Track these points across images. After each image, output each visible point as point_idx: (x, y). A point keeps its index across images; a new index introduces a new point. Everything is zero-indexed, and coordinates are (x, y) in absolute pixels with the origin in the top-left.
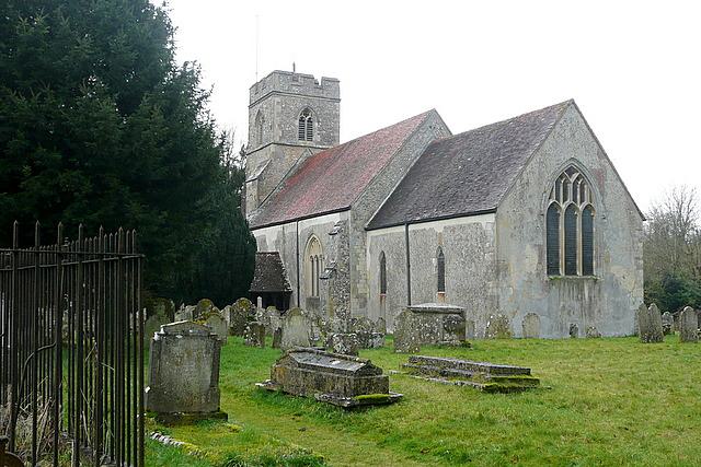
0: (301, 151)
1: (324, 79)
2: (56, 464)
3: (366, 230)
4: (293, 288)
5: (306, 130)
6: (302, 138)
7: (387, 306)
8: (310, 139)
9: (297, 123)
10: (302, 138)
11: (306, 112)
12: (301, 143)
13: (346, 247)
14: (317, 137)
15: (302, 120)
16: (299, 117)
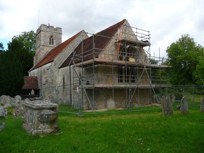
0: (50, 48)
1: (57, 28)
2: (1, 132)
3: (59, 68)
4: (40, 88)
5: (51, 42)
6: (50, 44)
7: (65, 94)
8: (53, 44)
9: (49, 40)
10: (50, 44)
11: (51, 37)
12: (50, 45)
13: (52, 74)
14: (55, 44)
15: (50, 39)
16: (49, 38)
